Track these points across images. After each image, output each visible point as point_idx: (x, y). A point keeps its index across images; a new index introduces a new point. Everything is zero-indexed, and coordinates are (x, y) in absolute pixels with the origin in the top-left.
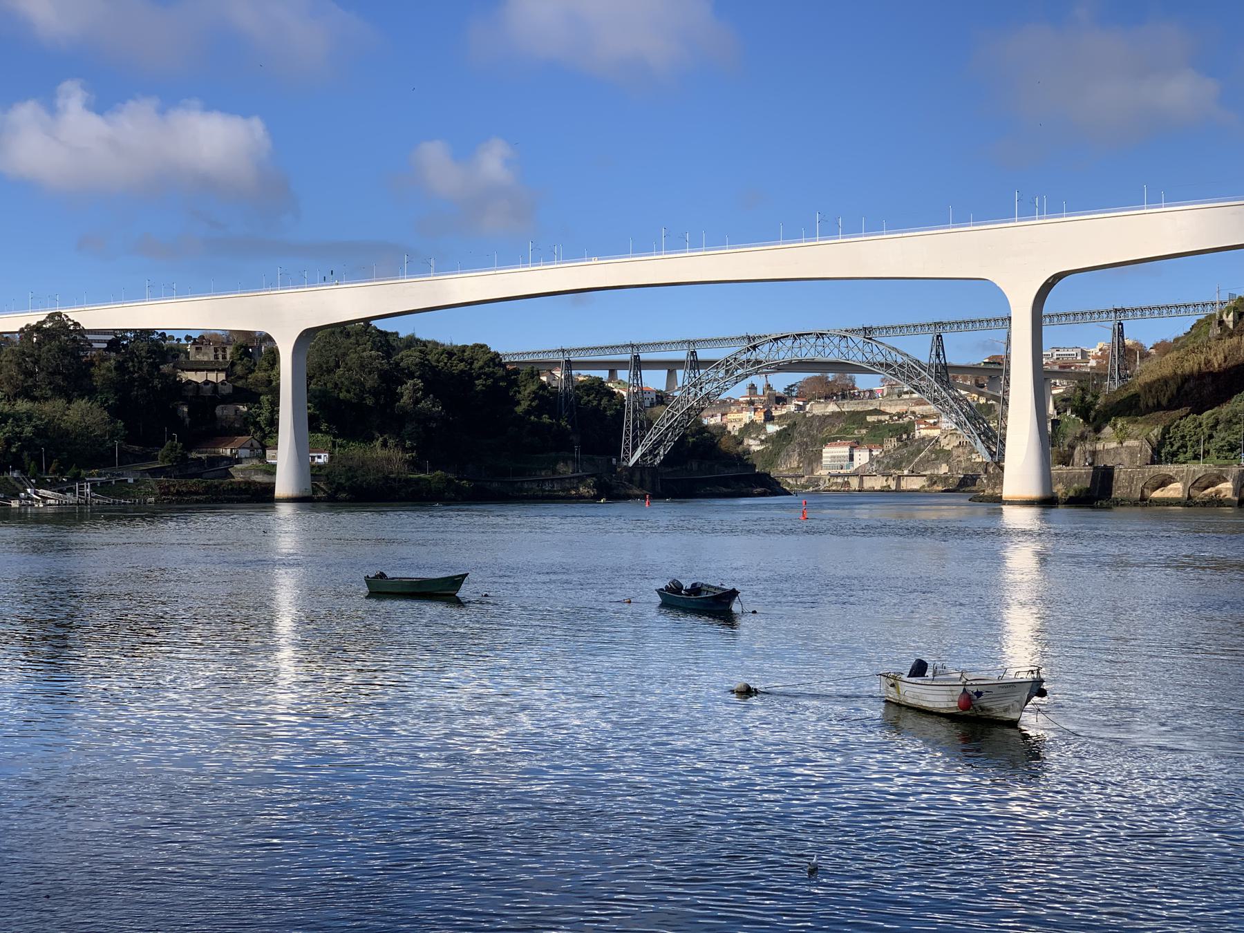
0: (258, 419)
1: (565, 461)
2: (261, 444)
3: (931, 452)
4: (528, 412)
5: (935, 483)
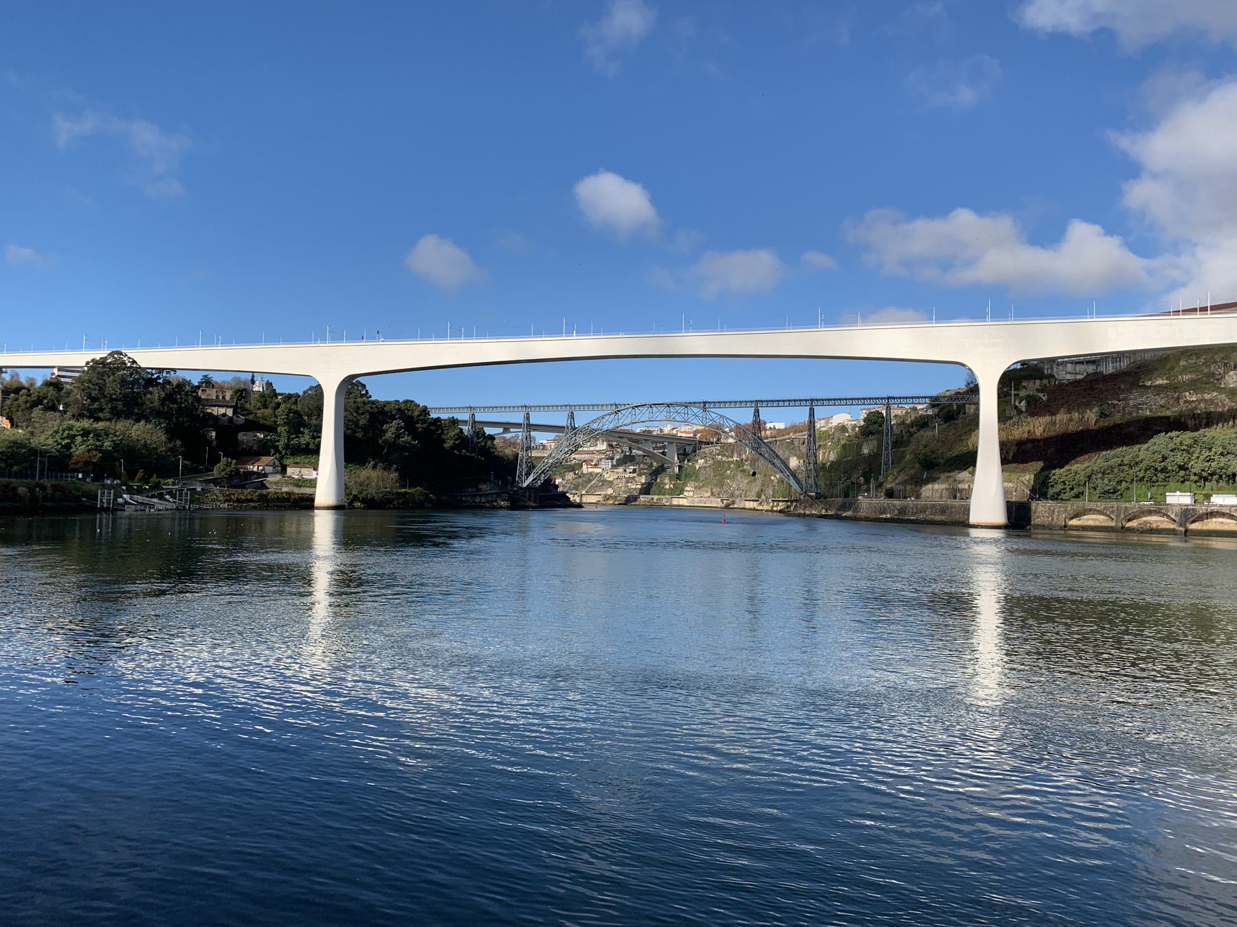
0: (278, 444)
1: (485, 482)
2: (281, 463)
3: (599, 481)
4: (452, 448)
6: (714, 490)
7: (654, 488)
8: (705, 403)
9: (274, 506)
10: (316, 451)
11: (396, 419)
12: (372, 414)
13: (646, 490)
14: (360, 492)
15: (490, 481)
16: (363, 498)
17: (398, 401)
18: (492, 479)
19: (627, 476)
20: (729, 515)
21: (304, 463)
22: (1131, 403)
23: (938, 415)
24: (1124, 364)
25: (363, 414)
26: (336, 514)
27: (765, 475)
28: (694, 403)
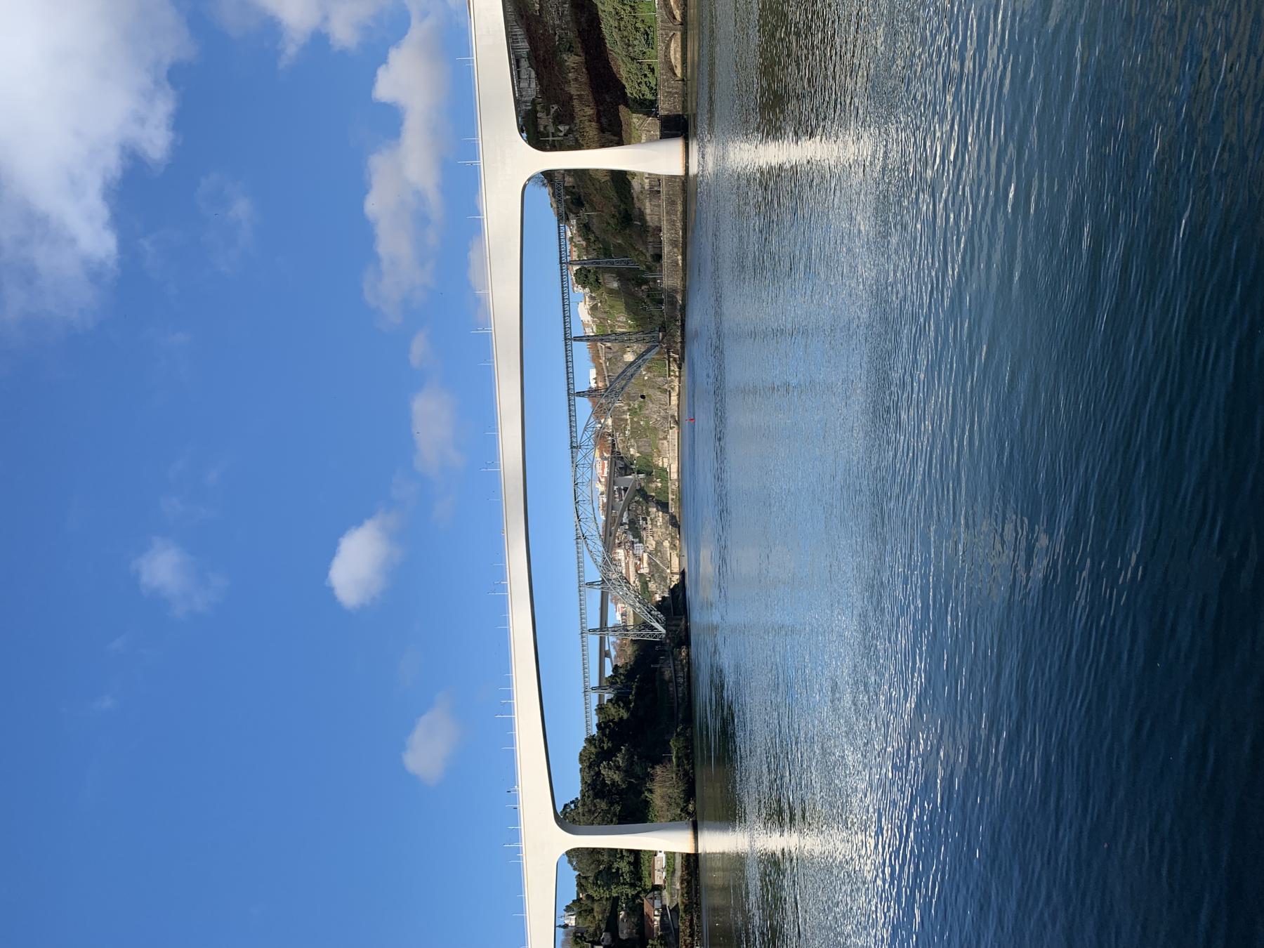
1: (662, 674)
2: (651, 891)
4: (628, 710)
5: (674, 545)
6: (661, 437)
7: (664, 500)
8: (572, 447)
9: (696, 896)
10: (636, 853)
11: (600, 771)
12: (596, 796)
13: (663, 506)
14: (678, 805)
15: (660, 668)
16: (685, 802)
17: (581, 770)
18: (658, 666)
19: (650, 527)
20: (686, 424)
21: (650, 866)
22: (557, 22)
23: (576, 214)
24: (519, 31)
25: (595, 806)
26: (702, 829)
27: (644, 385)
28: (572, 458)
